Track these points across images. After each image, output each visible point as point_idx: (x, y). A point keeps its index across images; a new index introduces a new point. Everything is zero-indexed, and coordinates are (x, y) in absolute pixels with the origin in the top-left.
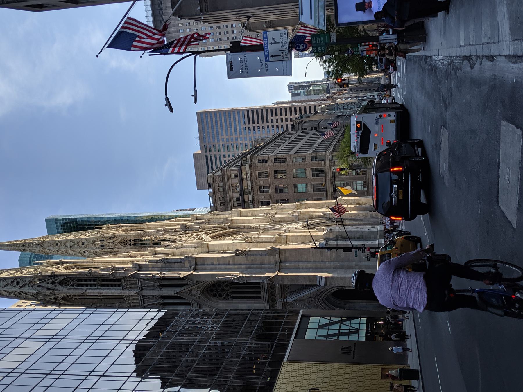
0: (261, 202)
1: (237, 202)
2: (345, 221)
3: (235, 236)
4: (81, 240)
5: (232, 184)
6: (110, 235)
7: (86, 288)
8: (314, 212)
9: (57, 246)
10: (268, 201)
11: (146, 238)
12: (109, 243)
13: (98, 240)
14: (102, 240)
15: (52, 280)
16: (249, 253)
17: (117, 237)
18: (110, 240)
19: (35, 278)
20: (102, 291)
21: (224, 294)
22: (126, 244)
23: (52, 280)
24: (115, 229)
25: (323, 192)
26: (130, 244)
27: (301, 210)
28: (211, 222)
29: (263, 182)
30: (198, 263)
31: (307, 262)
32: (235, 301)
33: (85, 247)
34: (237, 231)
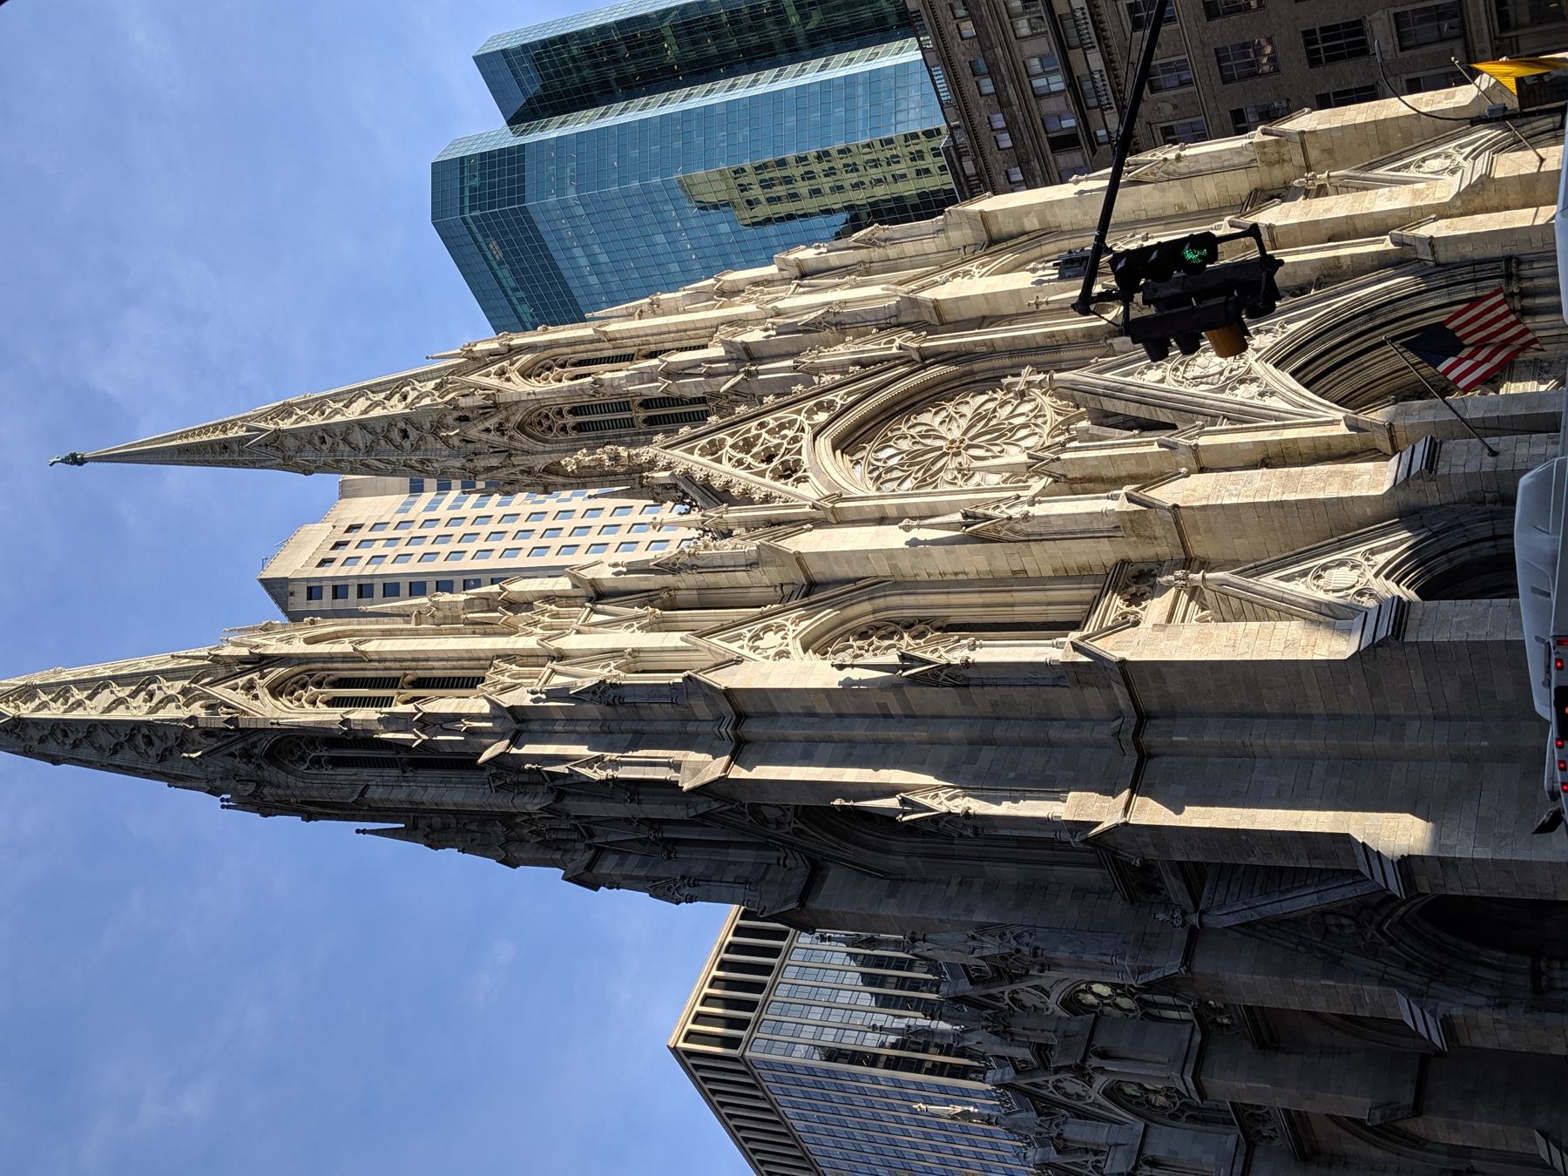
2: (1528, 273)
3: (950, 407)
4: (391, 421)
6: (477, 400)
7: (366, 773)
9: (324, 447)
11: (578, 462)
12: (488, 430)
13: (450, 420)
15: (241, 745)
16: (970, 673)
17: (507, 406)
18: (486, 419)
22: (550, 429)
23: (241, 745)
26: (564, 429)
28: (847, 320)
31: (1294, 716)
33: (416, 448)
34: (964, 375)
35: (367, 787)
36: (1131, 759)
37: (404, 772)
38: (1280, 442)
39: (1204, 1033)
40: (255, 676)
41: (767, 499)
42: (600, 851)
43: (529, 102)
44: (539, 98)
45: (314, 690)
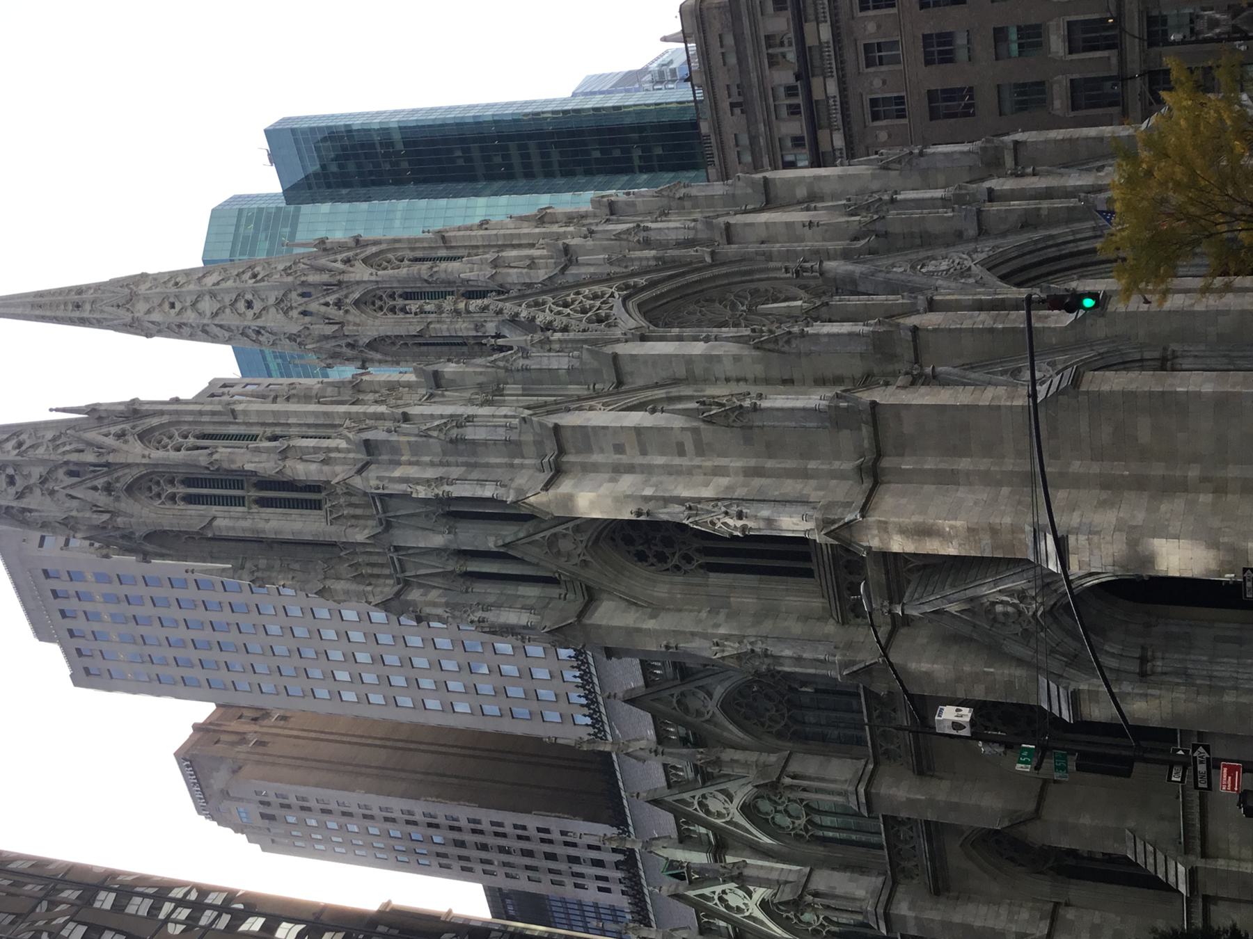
0: (871, 100)
1: (788, 102)
5: (768, 37)
7: (215, 510)
8: (1048, 194)
10: (896, 98)
12: (327, 304)
14: (303, 295)
15: (106, 479)
17: (349, 284)
19: (56, 467)
20: (261, 525)
21: (674, 554)
23: (106, 479)
24: (344, 255)
25: (1105, 53)
26: (393, 310)
27: (995, 184)
29: (879, 27)
30: (569, 446)
32: (714, 578)
33: (257, 316)
35: (214, 518)
36: (867, 484)
37: (250, 508)
38: (992, 300)
39: (876, 764)
40: (127, 426)
41: (584, 331)
42: (406, 584)
43: (307, 177)
44: (316, 175)
45: (180, 440)
